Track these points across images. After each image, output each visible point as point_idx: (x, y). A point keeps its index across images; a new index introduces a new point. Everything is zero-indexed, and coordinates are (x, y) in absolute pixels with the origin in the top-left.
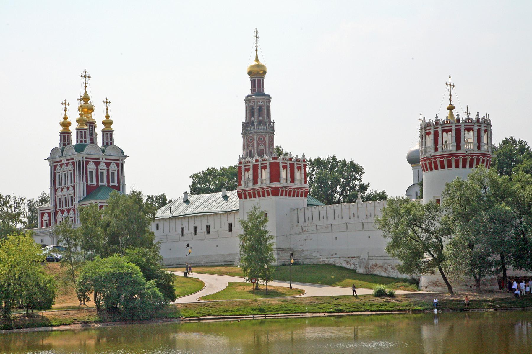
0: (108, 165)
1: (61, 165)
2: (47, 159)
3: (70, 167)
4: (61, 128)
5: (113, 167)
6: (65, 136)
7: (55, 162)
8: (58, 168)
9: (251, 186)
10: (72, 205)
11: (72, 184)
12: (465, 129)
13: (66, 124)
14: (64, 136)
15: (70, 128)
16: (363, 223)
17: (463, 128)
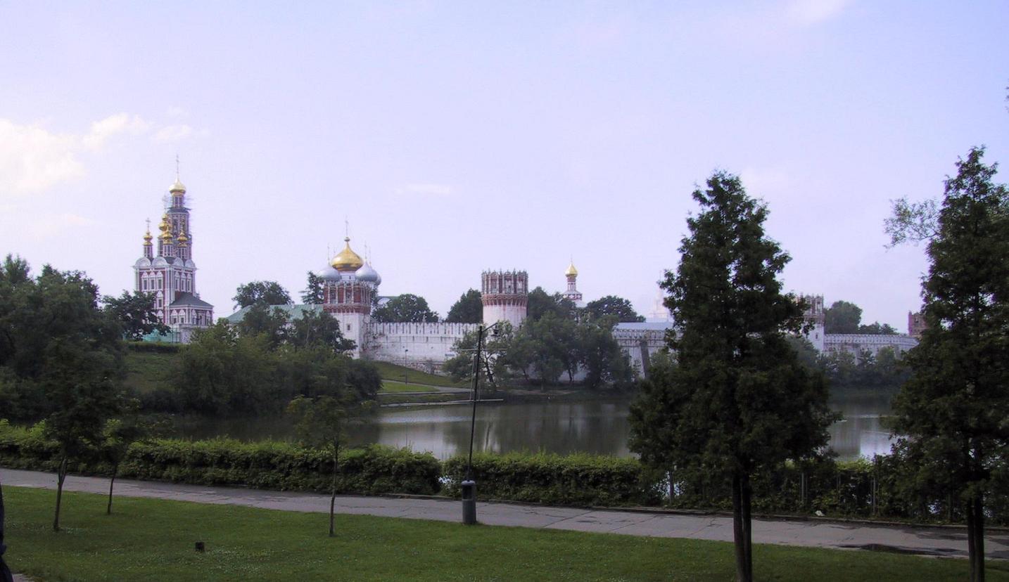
0: (186, 274)
1: (149, 273)
2: (134, 267)
3: (160, 275)
4: (144, 242)
5: (189, 275)
6: (148, 248)
7: (140, 269)
8: (145, 276)
9: (336, 303)
10: (160, 306)
11: (162, 289)
12: (519, 280)
13: (149, 239)
14: (148, 248)
15: (152, 241)
16: (427, 338)
17: (518, 279)
